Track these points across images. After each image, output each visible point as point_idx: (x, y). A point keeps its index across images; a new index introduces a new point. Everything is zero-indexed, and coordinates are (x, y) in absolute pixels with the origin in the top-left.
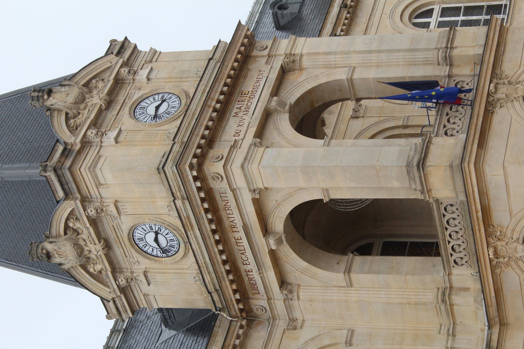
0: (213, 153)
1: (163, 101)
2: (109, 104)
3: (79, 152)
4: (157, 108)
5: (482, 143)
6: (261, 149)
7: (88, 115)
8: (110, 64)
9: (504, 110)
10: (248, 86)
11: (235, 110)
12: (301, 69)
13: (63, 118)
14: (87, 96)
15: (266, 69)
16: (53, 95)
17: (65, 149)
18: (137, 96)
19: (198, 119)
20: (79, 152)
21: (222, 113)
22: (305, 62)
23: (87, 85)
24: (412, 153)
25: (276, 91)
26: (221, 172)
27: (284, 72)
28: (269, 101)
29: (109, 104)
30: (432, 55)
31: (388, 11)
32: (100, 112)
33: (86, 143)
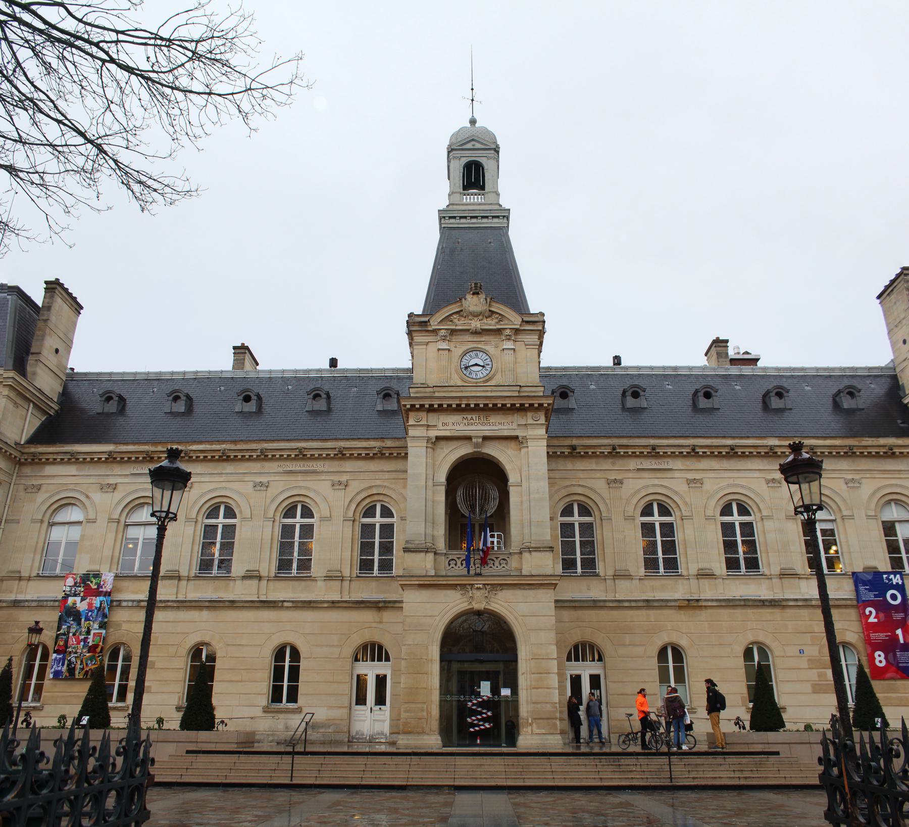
0: (423, 414)
1: (483, 367)
2: (476, 333)
3: (428, 331)
4: (476, 365)
5: (422, 586)
6: (425, 444)
7: (460, 324)
8: (512, 319)
9: (461, 597)
10: (494, 419)
11: (469, 417)
12: (520, 449)
13: (457, 310)
14: (480, 317)
15: (515, 426)
16: (475, 297)
17: (426, 322)
18: (487, 348)
19: (444, 397)
20: (428, 331)
21: (459, 409)
22: (523, 450)
23: (493, 312)
24: (417, 542)
25: (485, 438)
26: (421, 423)
27: (516, 438)
28: (477, 437)
29: (476, 333)
30: (527, 539)
31: (737, 482)
32: (468, 330)
33: (435, 331)
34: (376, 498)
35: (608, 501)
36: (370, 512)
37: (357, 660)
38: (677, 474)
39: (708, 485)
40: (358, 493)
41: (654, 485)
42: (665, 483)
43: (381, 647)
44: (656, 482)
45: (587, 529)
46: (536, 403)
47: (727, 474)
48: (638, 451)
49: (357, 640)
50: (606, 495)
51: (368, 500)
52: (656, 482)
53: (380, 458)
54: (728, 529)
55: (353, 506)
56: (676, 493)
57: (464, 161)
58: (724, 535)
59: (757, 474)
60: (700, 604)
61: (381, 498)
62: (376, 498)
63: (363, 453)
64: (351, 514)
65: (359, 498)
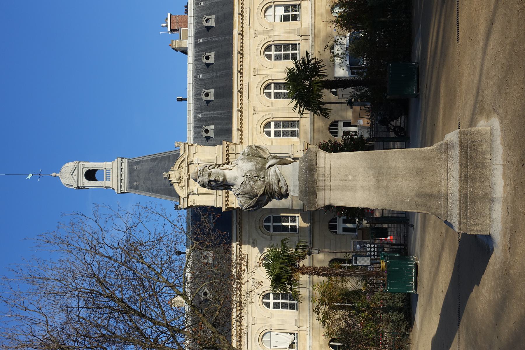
34: (261, 225)
35: (264, 114)
36: (268, 228)
37: (336, 232)
38: (251, 80)
39: (257, 66)
40: (259, 234)
41: (257, 91)
42: (255, 86)
43: (330, 222)
44: (255, 90)
45: (277, 124)
46: (225, 149)
47: (251, 54)
48: (240, 98)
49: (328, 232)
50: (261, 115)
51: (262, 229)
52: (255, 90)
53: (241, 224)
54: (278, 57)
55: (265, 236)
56: (260, 81)
57: (85, 180)
58: (280, 59)
59: (252, 41)
60: (313, 24)
61: (261, 222)
62: (261, 225)
63: (239, 231)
64: (269, 237)
65: (261, 233)
